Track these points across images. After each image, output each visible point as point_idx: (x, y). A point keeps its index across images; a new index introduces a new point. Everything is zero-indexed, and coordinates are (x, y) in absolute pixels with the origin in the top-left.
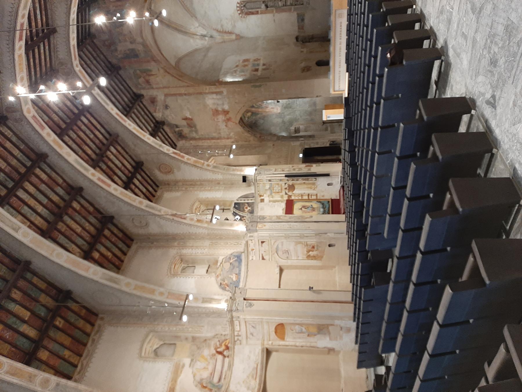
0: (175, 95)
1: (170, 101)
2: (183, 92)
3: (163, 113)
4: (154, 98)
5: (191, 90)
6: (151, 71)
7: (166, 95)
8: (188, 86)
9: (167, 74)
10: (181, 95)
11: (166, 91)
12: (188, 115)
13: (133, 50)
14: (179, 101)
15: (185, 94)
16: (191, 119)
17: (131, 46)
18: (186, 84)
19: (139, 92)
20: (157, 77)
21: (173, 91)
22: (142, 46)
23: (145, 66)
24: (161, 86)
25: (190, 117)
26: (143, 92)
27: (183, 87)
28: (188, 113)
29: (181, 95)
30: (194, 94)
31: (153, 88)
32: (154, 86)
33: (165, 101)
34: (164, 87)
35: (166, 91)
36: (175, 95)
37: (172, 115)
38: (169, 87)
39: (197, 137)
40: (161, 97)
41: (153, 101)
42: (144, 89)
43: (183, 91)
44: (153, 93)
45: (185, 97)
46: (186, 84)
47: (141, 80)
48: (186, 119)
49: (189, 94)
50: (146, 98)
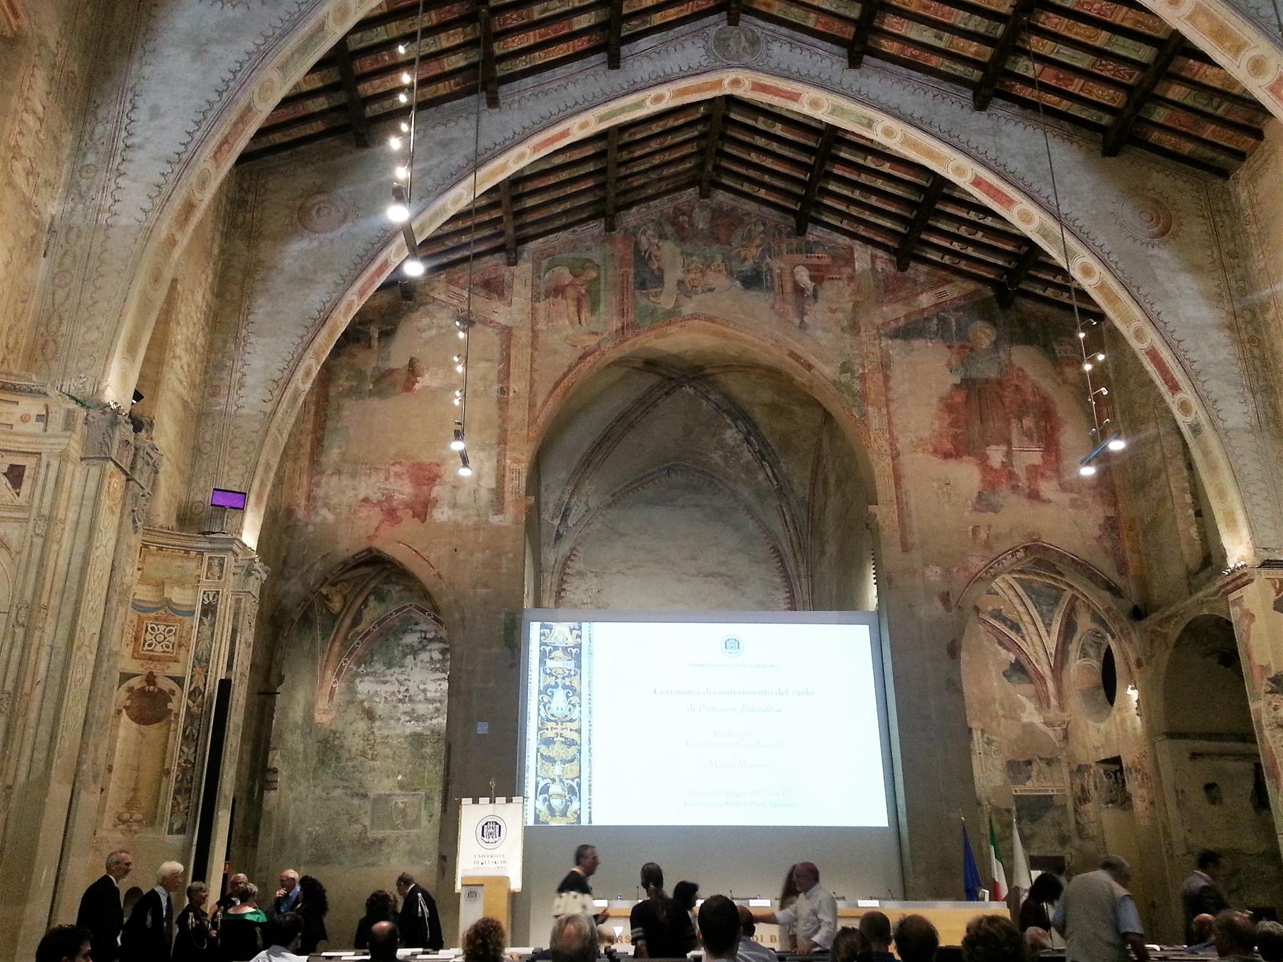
0: (506, 359)
1: (488, 339)
2: (514, 386)
3: (445, 305)
4: (501, 294)
5: (518, 414)
6: (594, 308)
7: (507, 333)
8: (532, 406)
9: (580, 353)
10: (505, 376)
11: (523, 336)
12: (424, 381)
13: (660, 280)
14: (483, 365)
15: (503, 391)
16: (408, 387)
17: (671, 278)
18: (539, 404)
19: (525, 255)
20: (571, 323)
21: (521, 357)
22: (670, 306)
23: (608, 302)
24: (541, 326)
25: (417, 386)
26: (524, 268)
27: (532, 392)
28: (435, 384)
29: (505, 376)
30: (504, 419)
31: (535, 298)
32: (541, 306)
33: (486, 322)
34: (535, 334)
35: (523, 336)
36: (506, 359)
37: (434, 332)
38: (534, 346)
39: (333, 392)
40: (502, 313)
41: (494, 288)
42: (537, 273)
43: (518, 385)
44: (521, 296)
45: (496, 387)
46: (539, 404)
47: (565, 275)
48: (413, 370)
49: (503, 403)
50: (506, 272)
